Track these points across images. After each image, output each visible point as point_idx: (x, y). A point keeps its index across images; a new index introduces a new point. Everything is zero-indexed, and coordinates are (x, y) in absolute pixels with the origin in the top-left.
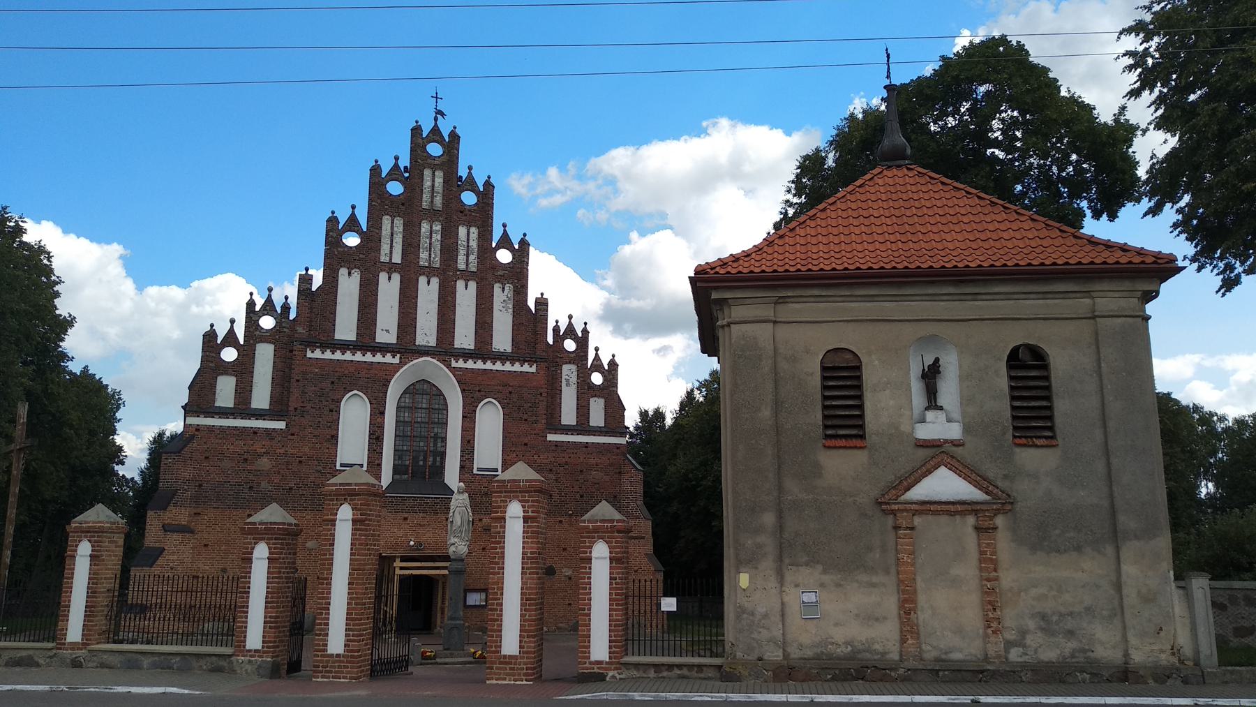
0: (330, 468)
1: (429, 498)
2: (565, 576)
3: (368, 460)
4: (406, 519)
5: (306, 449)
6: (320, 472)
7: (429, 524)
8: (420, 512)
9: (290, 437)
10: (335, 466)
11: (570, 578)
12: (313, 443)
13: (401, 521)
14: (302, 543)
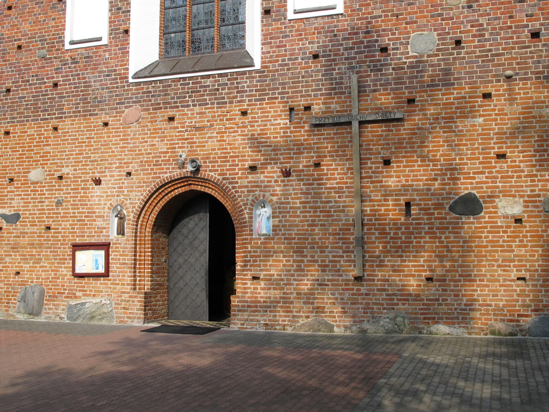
0: (58, 50)
1: (208, 76)
2: (506, 217)
3: (110, 26)
4: (171, 119)
5: (26, 27)
6: (44, 58)
7: (212, 125)
8: (194, 105)
9: (9, 12)
10: (63, 45)
11: (518, 221)
12: (35, 15)
13: (165, 125)
14: (24, 173)
